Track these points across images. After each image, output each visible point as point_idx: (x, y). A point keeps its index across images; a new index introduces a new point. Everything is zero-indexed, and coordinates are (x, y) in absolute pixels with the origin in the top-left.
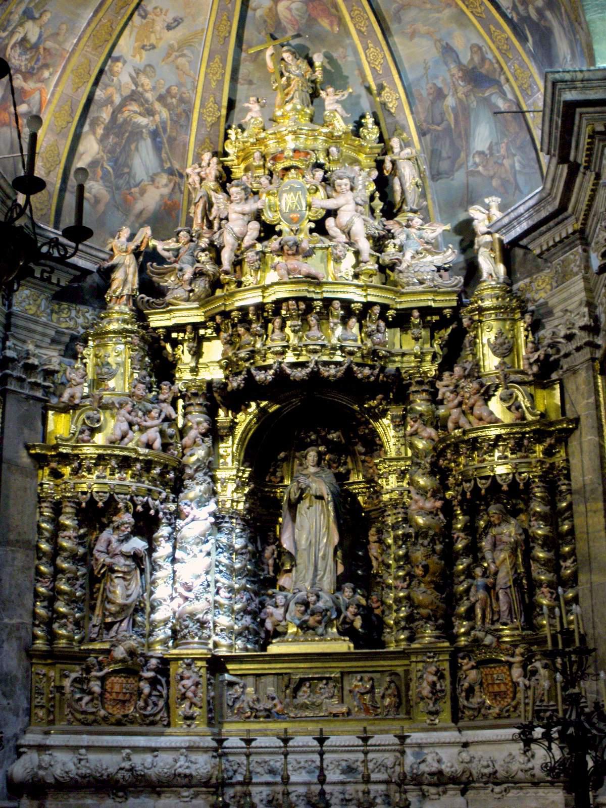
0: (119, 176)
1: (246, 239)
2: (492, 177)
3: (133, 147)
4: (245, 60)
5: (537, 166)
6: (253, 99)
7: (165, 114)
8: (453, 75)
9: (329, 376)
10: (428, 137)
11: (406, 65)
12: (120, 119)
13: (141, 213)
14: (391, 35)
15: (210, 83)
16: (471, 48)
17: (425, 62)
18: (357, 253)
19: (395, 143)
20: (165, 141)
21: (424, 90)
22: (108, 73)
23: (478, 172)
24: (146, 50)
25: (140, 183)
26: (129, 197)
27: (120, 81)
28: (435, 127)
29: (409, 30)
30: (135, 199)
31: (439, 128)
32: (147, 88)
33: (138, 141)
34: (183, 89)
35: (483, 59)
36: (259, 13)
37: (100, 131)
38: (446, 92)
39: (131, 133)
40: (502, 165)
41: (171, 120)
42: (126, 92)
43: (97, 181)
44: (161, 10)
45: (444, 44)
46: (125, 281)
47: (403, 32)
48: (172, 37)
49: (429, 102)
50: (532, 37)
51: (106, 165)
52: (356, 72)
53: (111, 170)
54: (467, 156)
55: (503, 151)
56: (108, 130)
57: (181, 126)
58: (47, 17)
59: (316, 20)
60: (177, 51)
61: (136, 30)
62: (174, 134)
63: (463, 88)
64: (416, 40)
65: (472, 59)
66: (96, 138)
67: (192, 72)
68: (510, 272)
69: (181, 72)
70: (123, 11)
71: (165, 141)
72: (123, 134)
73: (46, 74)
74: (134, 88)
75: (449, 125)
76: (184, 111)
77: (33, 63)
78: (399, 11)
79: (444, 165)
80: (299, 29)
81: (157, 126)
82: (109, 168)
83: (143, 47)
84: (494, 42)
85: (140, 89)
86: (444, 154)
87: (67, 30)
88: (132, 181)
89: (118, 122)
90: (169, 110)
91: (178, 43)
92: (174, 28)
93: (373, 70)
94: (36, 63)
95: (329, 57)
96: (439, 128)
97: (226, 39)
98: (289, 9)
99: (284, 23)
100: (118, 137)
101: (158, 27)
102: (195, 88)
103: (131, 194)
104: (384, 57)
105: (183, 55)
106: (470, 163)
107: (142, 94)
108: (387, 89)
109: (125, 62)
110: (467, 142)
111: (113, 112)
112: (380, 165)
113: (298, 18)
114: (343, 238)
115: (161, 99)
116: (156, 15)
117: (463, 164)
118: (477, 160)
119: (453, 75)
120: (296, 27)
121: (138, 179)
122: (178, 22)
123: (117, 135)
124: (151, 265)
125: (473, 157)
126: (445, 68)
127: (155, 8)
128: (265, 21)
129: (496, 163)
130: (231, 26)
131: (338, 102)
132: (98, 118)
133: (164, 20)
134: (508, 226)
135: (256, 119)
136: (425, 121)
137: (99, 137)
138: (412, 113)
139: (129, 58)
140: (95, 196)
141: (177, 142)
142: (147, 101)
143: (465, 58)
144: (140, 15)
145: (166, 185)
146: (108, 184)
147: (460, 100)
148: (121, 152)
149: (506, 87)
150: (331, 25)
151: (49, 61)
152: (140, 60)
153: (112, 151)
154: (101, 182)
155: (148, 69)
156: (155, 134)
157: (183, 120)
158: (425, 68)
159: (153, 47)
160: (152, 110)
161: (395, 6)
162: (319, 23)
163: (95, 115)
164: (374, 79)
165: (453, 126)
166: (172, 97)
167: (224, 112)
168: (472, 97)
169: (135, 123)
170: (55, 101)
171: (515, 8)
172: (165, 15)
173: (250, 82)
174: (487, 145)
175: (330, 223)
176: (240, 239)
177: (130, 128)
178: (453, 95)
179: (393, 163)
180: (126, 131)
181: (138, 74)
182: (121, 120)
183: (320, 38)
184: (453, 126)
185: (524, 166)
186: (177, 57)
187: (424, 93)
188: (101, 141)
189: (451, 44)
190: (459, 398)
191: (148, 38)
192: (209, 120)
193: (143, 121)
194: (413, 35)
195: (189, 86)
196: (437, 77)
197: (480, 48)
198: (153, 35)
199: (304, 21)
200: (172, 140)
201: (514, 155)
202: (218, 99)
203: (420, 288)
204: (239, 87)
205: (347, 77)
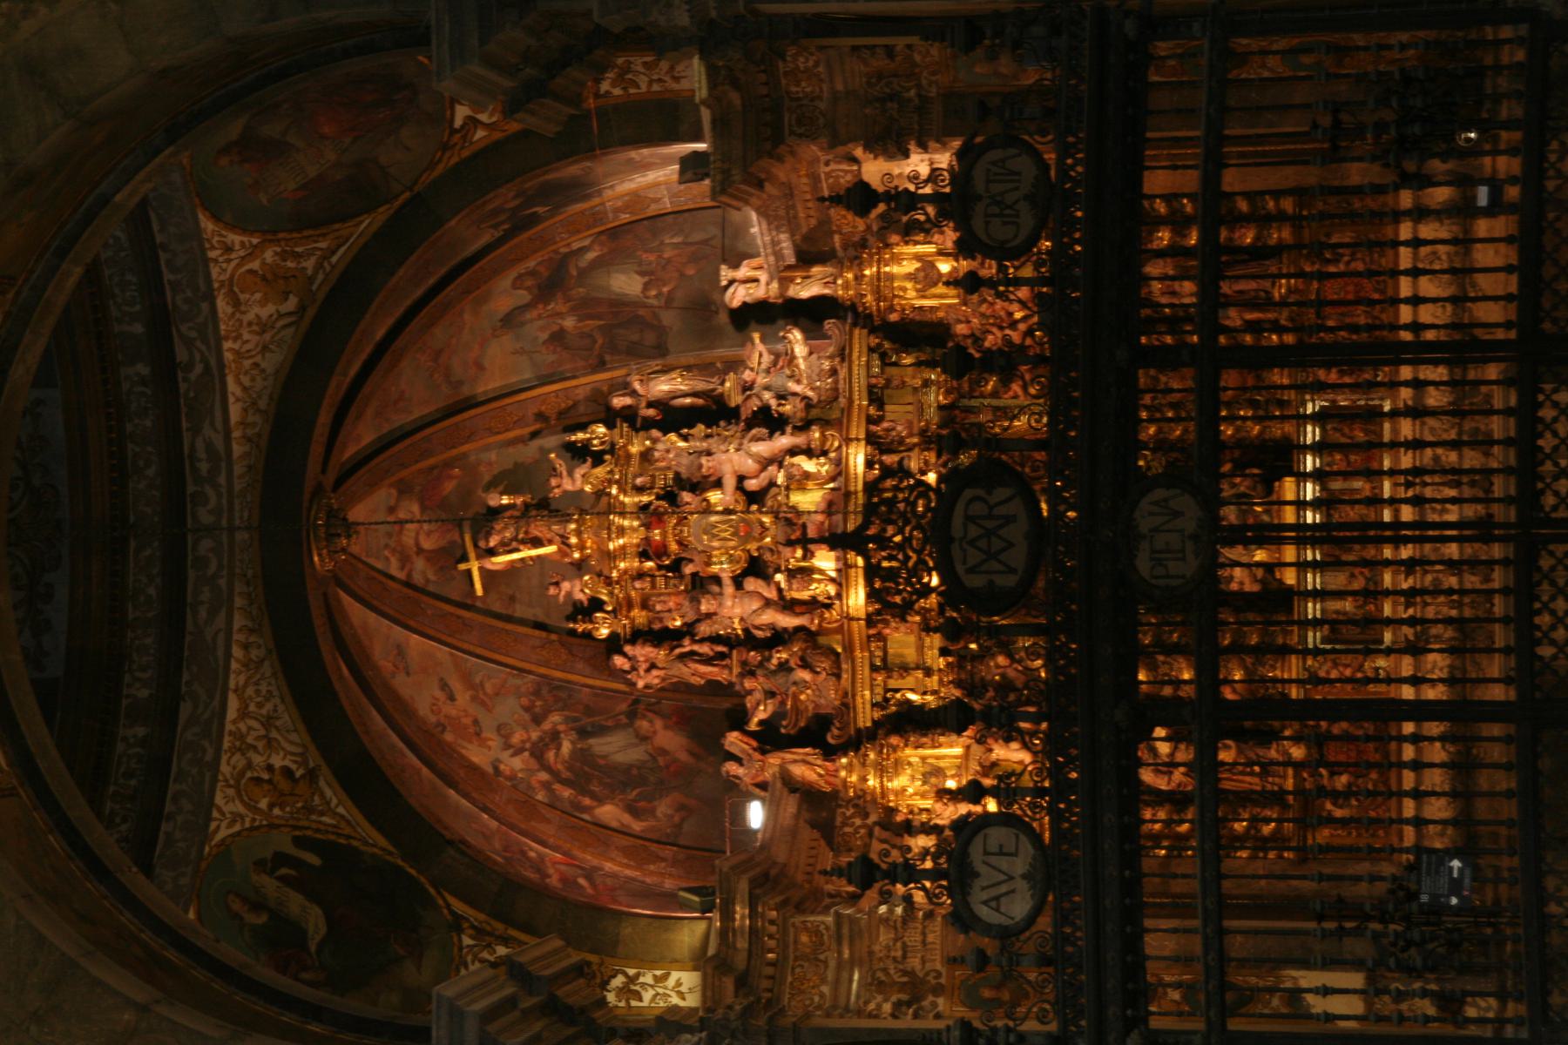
1: (766, 594)
2: (682, 275)
3: (602, 762)
5: (686, 215)
6: (552, 591)
7: (555, 718)
10: (608, 358)
12: (566, 774)
13: (692, 754)
14: (474, 397)
17: (515, 352)
18: (793, 451)
19: (619, 402)
21: (548, 357)
25: (651, 755)
26: (672, 769)
27: (521, 770)
28: (597, 346)
34: (523, 689)
35: (532, 273)
36: (432, 577)
37: (587, 801)
38: (555, 328)
40: (669, 261)
41: (562, 709)
42: (533, 764)
45: (499, 324)
52: (511, 450)
53: (638, 790)
54: (645, 306)
55: (652, 258)
56: (584, 792)
61: (460, 741)
63: (557, 305)
65: (528, 289)
74: (526, 754)
75: (600, 327)
79: (650, 338)
81: (572, 729)
82: (634, 793)
83: (478, 734)
85: (528, 745)
86: (635, 337)
90: (550, 712)
92: (451, 691)
95: (492, 485)
96: (600, 341)
98: (429, 534)
99: (443, 543)
101: (454, 713)
103: (667, 767)
105: (482, 685)
106: (654, 302)
112: (648, 424)
114: (772, 469)
115: (537, 720)
117: (654, 313)
118: (653, 293)
119: (540, 317)
121: (647, 757)
122: (444, 686)
124: (785, 727)
125: (647, 297)
127: (432, 711)
129: (664, 268)
131: (571, 474)
132: (571, 803)
134: (778, 255)
135: (586, 585)
137: (595, 804)
138: (574, 377)
140: (677, 810)
142: (541, 739)
143: (523, 296)
145: (651, 722)
147: (573, 310)
149: (575, 246)
150: (451, 477)
152: (495, 742)
154: (656, 803)
155: (503, 732)
156: (583, 733)
157: (563, 695)
159: (476, 722)
164: (527, 425)
166: (534, 706)
168: (574, 292)
170: (567, 846)
171: (495, 227)
173: (512, 599)
174: (638, 277)
175: (752, 484)
176: (768, 603)
177: (578, 764)
179: (650, 405)
186: (485, 694)
187: (551, 358)
188: (601, 801)
189: (500, 316)
190: (995, 330)
193: (566, 747)
194: (480, 367)
196: (536, 338)
197: (520, 276)
200: (589, 711)
201: (662, 243)
203: (843, 373)
204: (518, 614)
205: (516, 464)
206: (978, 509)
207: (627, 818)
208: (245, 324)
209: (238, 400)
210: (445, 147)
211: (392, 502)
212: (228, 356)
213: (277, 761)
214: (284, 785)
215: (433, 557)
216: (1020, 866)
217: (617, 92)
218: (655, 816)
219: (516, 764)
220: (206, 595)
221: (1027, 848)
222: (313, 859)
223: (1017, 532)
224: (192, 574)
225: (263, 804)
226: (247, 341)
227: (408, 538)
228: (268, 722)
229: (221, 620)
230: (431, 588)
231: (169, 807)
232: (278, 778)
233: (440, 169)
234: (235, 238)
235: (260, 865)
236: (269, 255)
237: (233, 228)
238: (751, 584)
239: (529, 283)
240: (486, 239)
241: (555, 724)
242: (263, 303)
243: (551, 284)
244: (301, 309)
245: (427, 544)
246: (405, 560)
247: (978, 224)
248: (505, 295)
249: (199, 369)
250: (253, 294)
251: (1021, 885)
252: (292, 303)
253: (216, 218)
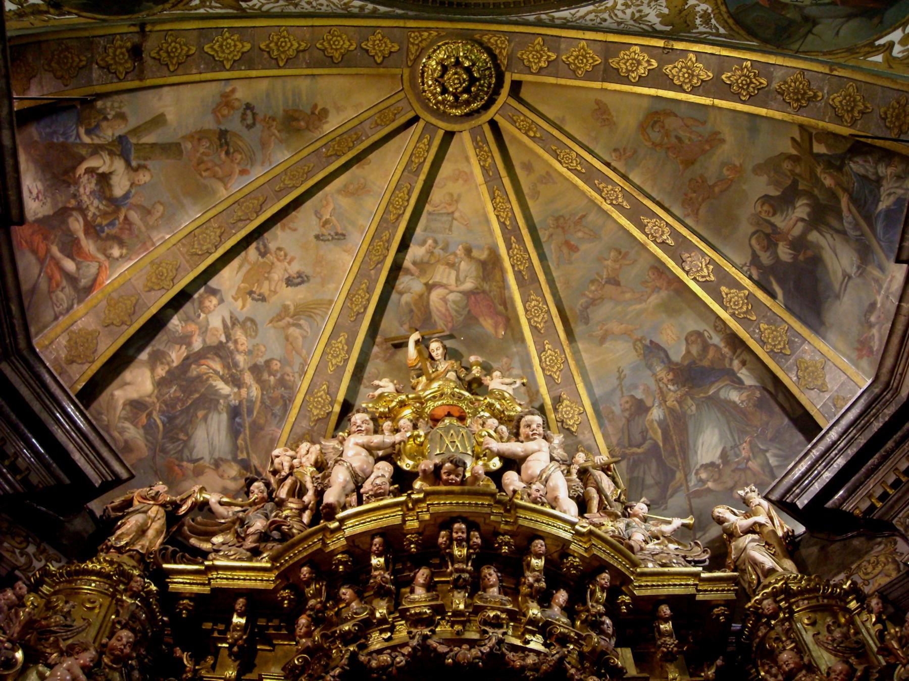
4: (377, 357)
7: (255, 391)
8: (661, 380)
9: (523, 668)
12: (194, 371)
15: (327, 366)
16: (686, 339)
17: (620, 372)
20: (247, 425)
21: (618, 407)
22: (196, 304)
23: (709, 490)
24: (253, 299)
29: (599, 332)
30: (185, 476)
31: (640, 451)
32: (241, 348)
33: (209, 410)
34: (288, 369)
35: (706, 347)
36: (406, 298)
37: (161, 371)
38: (648, 403)
39: (203, 396)
41: (262, 402)
42: (212, 341)
43: (136, 426)
44: (286, 255)
45: (648, 342)
46: (142, 531)
47: (591, 336)
48: (291, 296)
49: (624, 421)
50: (782, 288)
51: (155, 415)
53: (161, 426)
57: (274, 415)
58: (144, 177)
59: (476, 319)
60: (292, 317)
62: (262, 421)
63: (673, 392)
64: (607, 345)
65: (688, 352)
66: (153, 377)
67: (304, 352)
69: (290, 347)
70: (240, 224)
71: (247, 425)
72: (191, 393)
73: (116, 252)
74: (223, 339)
75: (656, 445)
76: (282, 397)
77: (105, 223)
78: (587, 308)
80: (453, 329)
81: (241, 402)
83: (251, 293)
84: (725, 308)
85: (231, 345)
86: (649, 481)
87: (162, 216)
88: (186, 453)
89: (189, 374)
90: (262, 389)
91: (296, 306)
93: (549, 379)
94: (108, 225)
96: (640, 451)
97: (360, 315)
98: (444, 300)
99: (436, 317)
100: (184, 392)
102: (303, 373)
104: (566, 361)
105: (299, 326)
107: (231, 353)
108: (566, 402)
109: (221, 301)
110: (686, 459)
111: (187, 358)
113: (454, 313)
115: (255, 370)
116: (279, 260)
117: (681, 485)
118: (704, 476)
120: (450, 325)
121: (195, 456)
123: (183, 389)
125: (697, 473)
126: (649, 373)
127: (279, 249)
128: (411, 311)
130: (369, 300)
133: (286, 270)
136: (618, 445)
137: (157, 378)
139: (229, 295)
140: (126, 442)
141: (263, 433)
142: (236, 365)
143: (678, 353)
144: (257, 248)
145: (234, 479)
146: (150, 438)
147: (671, 410)
148: (182, 412)
150: (496, 327)
151: (125, 237)
152: (244, 308)
153: (170, 405)
154: (141, 431)
155: (249, 324)
157: (277, 409)
158: (619, 378)
159: (263, 299)
160: (239, 380)
161: (583, 301)
162: (481, 325)
163: (162, 347)
165: (661, 444)
166: (271, 373)
167: (337, 408)
168: (690, 402)
169: (211, 386)
172: (289, 263)
177: (203, 390)
178: (660, 405)
180: (196, 391)
181: (234, 324)
182: (195, 373)
184: (661, 444)
186: (289, 325)
187: (617, 410)
188: (161, 384)
189: (654, 340)
191: (260, 286)
192: (316, 412)
193: (224, 388)
194: (603, 340)
195: (296, 369)
196: (635, 387)
198: (266, 283)
199: (461, 319)
200: (256, 428)
202: (332, 390)
207: (131, 393)
208: (640, 8)
209: (573, 15)
211: (475, 253)
215: (423, 301)
218: (126, 419)
226: (624, 13)
227: (442, 274)
230: (394, 296)
239: (694, 350)
241: (248, 388)
245: (435, 296)
246: (423, 266)
250: (667, 7)
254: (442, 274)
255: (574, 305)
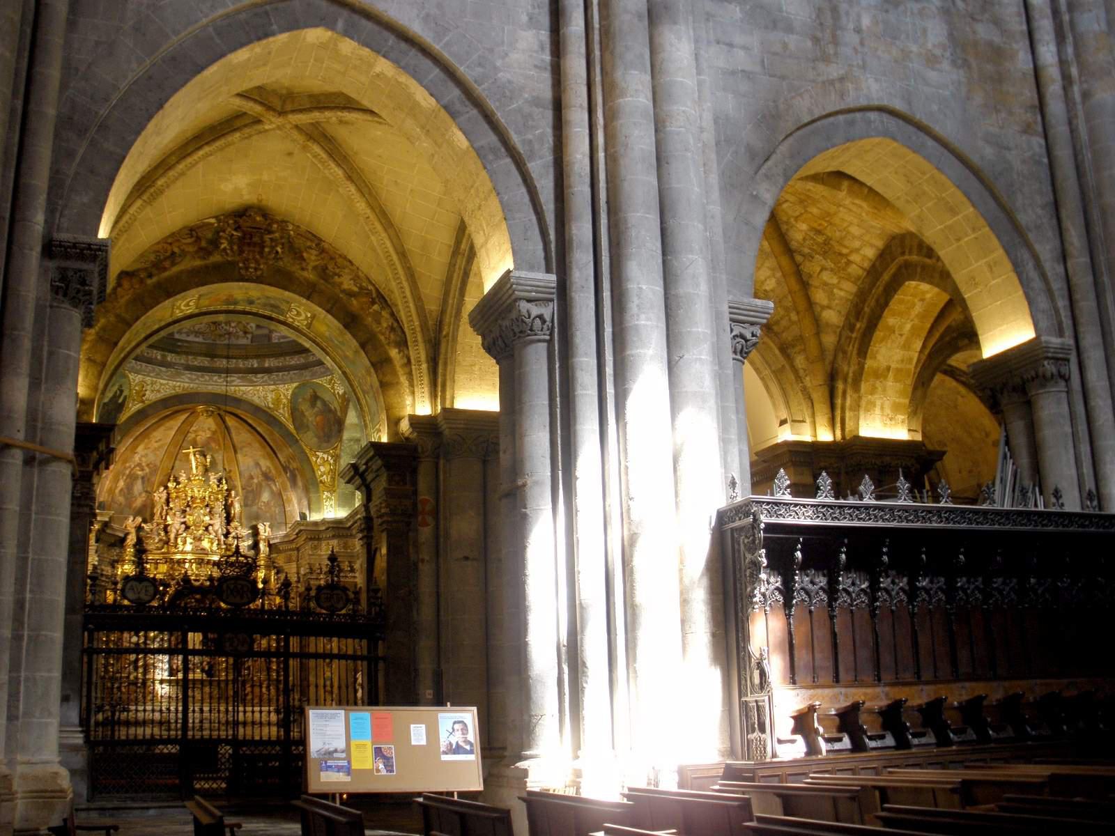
0: (129, 494)
7: (147, 470)
11: (241, 464)
18: (219, 540)
19: (233, 493)
21: (246, 474)
35: (270, 471)
63: (261, 478)
68: (270, 551)
79: (249, 503)
95: (212, 457)
112: (226, 500)
115: (148, 465)
122: (160, 440)
134: (273, 539)
143: (264, 469)
152: (143, 453)
156: (143, 478)
173: (181, 460)
175: (210, 528)
176: (178, 531)
183: (210, 449)
185: (280, 512)
188: (125, 481)
193: (140, 473)
194: (246, 455)
200: (149, 479)
206: (245, 589)
207: (119, 489)
210: (311, 449)
212: (258, 388)
213: (147, 393)
214: (141, 394)
216: (143, 596)
217: (324, 497)
219: (137, 458)
220: (194, 377)
221: (147, 598)
222: (120, 401)
223: (238, 600)
224: (199, 373)
225: (137, 388)
227: (200, 433)
228: (159, 391)
229: (187, 380)
231: (139, 363)
232: (142, 393)
233: (305, 447)
234: (290, 392)
235: (121, 386)
236: (284, 401)
237: (293, 392)
238: (183, 526)
240: (281, 459)
242: (272, 398)
243: (267, 477)
244: (269, 408)
246: (195, 431)
247: (325, 591)
248: (265, 464)
249: (255, 380)
251: (137, 596)
252: (271, 406)
253: (296, 388)
254: (200, 433)
255: (238, 445)
